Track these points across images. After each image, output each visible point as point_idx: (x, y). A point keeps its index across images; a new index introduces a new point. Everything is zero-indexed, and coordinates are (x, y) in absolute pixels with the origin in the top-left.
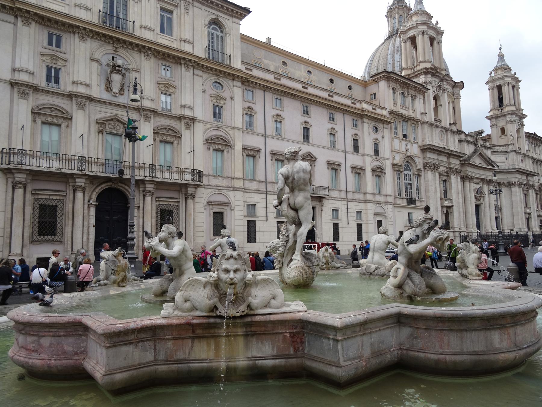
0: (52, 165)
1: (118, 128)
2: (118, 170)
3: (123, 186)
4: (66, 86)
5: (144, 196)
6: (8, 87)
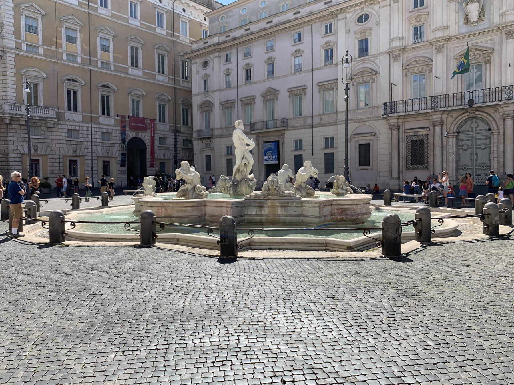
0: (413, 108)
1: (478, 56)
2: (468, 99)
3: (481, 113)
4: (429, 35)
5: (504, 120)
6: (388, 56)
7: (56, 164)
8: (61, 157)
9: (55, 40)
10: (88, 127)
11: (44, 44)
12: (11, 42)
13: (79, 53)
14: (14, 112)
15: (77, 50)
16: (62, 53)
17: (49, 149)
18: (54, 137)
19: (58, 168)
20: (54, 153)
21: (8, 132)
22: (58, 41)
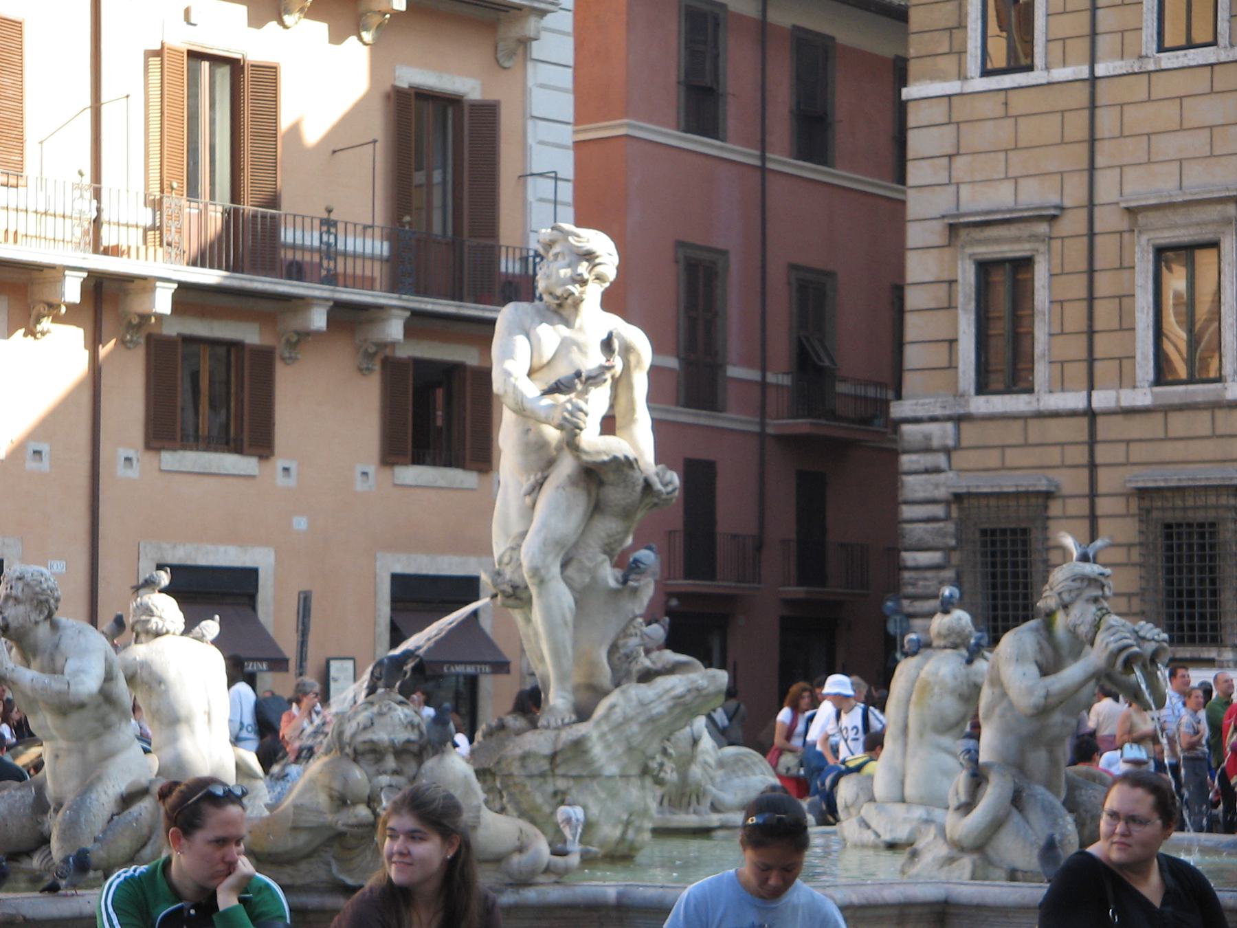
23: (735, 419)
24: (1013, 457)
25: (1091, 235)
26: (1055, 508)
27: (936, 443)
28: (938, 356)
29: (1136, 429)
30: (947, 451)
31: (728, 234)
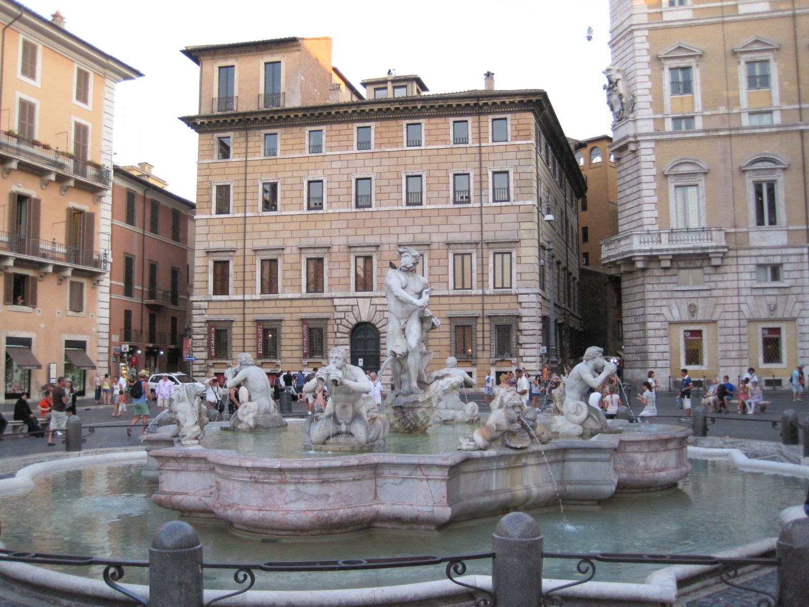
7: (733, 338)
8: (744, 323)
9: (724, 93)
10: (802, 255)
11: (705, 106)
12: (648, 122)
13: (776, 102)
14: (647, 247)
15: (771, 98)
16: (739, 114)
17: (720, 309)
18: (729, 285)
19: (737, 346)
20: (728, 316)
21: (643, 284)
22: (731, 94)
23: (136, 299)
24: (223, 311)
25: (244, 256)
26: (234, 324)
27: (202, 307)
28: (203, 285)
29: (256, 305)
30: (205, 309)
31: (136, 251)
